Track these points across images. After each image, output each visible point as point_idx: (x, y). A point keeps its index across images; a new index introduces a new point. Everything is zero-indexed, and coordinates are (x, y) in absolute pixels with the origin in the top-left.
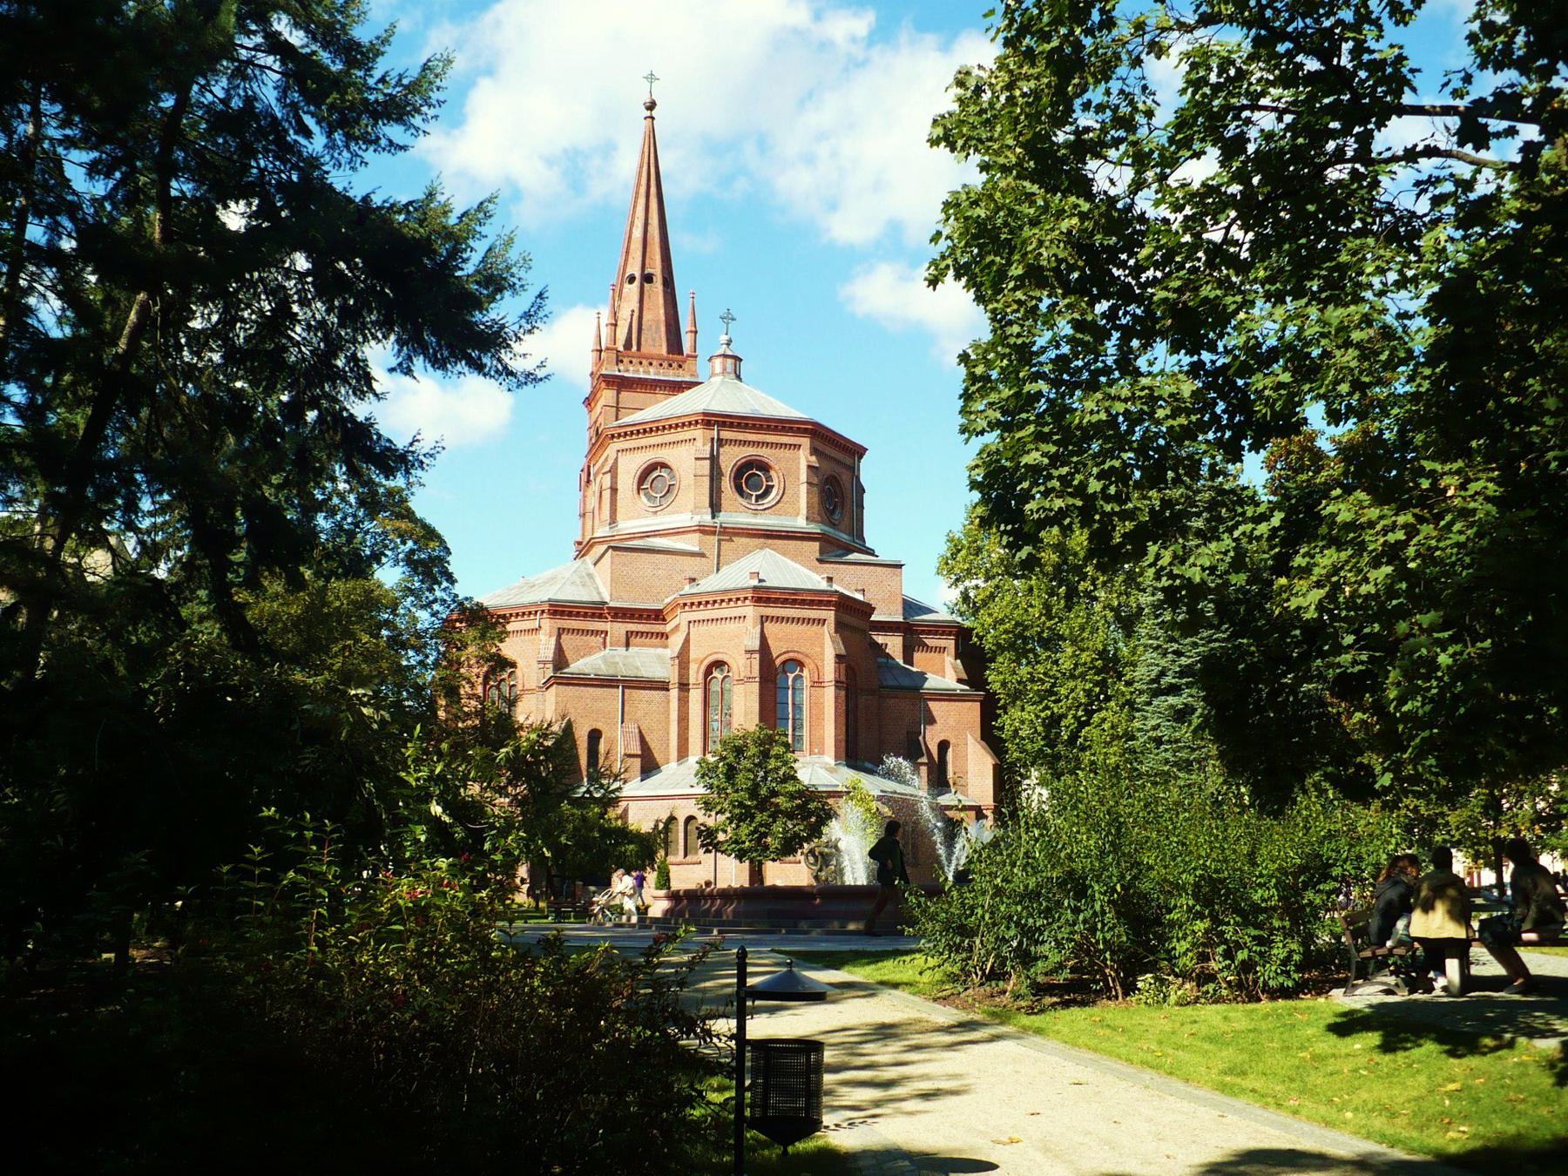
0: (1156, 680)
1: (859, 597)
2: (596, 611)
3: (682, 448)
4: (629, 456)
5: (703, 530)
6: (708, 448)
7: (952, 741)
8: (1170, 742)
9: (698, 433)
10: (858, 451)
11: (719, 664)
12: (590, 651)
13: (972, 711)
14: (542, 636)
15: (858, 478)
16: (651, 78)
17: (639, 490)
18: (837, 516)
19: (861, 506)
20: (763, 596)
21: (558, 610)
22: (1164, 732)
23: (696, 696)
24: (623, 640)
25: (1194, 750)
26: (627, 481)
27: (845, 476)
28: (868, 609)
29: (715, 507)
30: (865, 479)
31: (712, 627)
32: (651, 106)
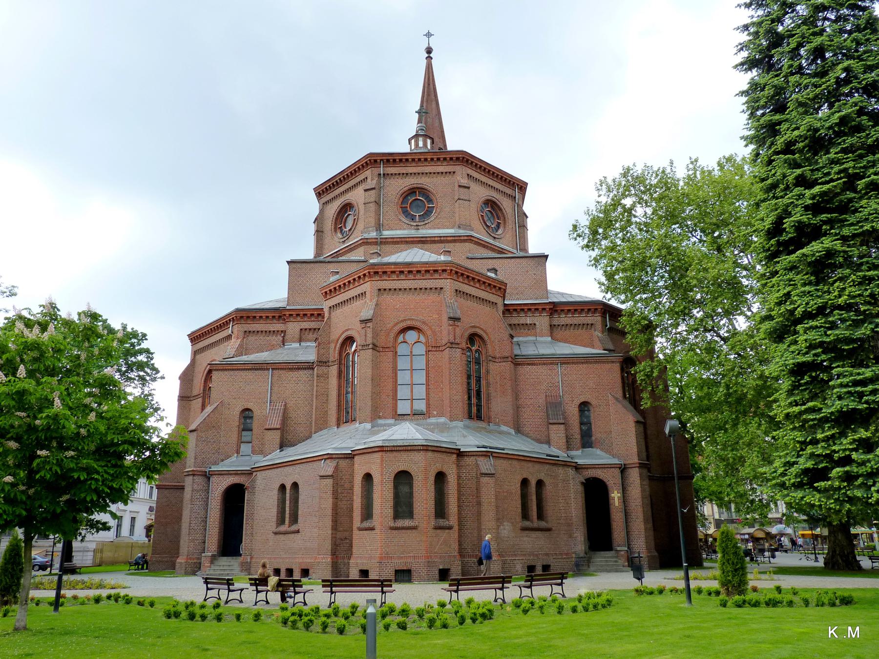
0: (776, 229)
1: (492, 275)
2: (278, 314)
3: (360, 190)
4: (330, 206)
5: (365, 242)
6: (375, 182)
7: (593, 402)
8: (808, 316)
9: (368, 173)
10: (522, 187)
11: (350, 340)
12: (271, 348)
13: (612, 373)
14: (233, 340)
15: (520, 206)
16: (429, 35)
17: (335, 231)
18: (500, 232)
19: (523, 227)
20: (378, 272)
21: (242, 316)
22: (800, 305)
23: (334, 370)
24: (297, 336)
25: (857, 324)
26: (329, 224)
27: (506, 204)
28: (500, 288)
29: (379, 227)
30: (526, 208)
31: (346, 309)
32: (429, 51)
